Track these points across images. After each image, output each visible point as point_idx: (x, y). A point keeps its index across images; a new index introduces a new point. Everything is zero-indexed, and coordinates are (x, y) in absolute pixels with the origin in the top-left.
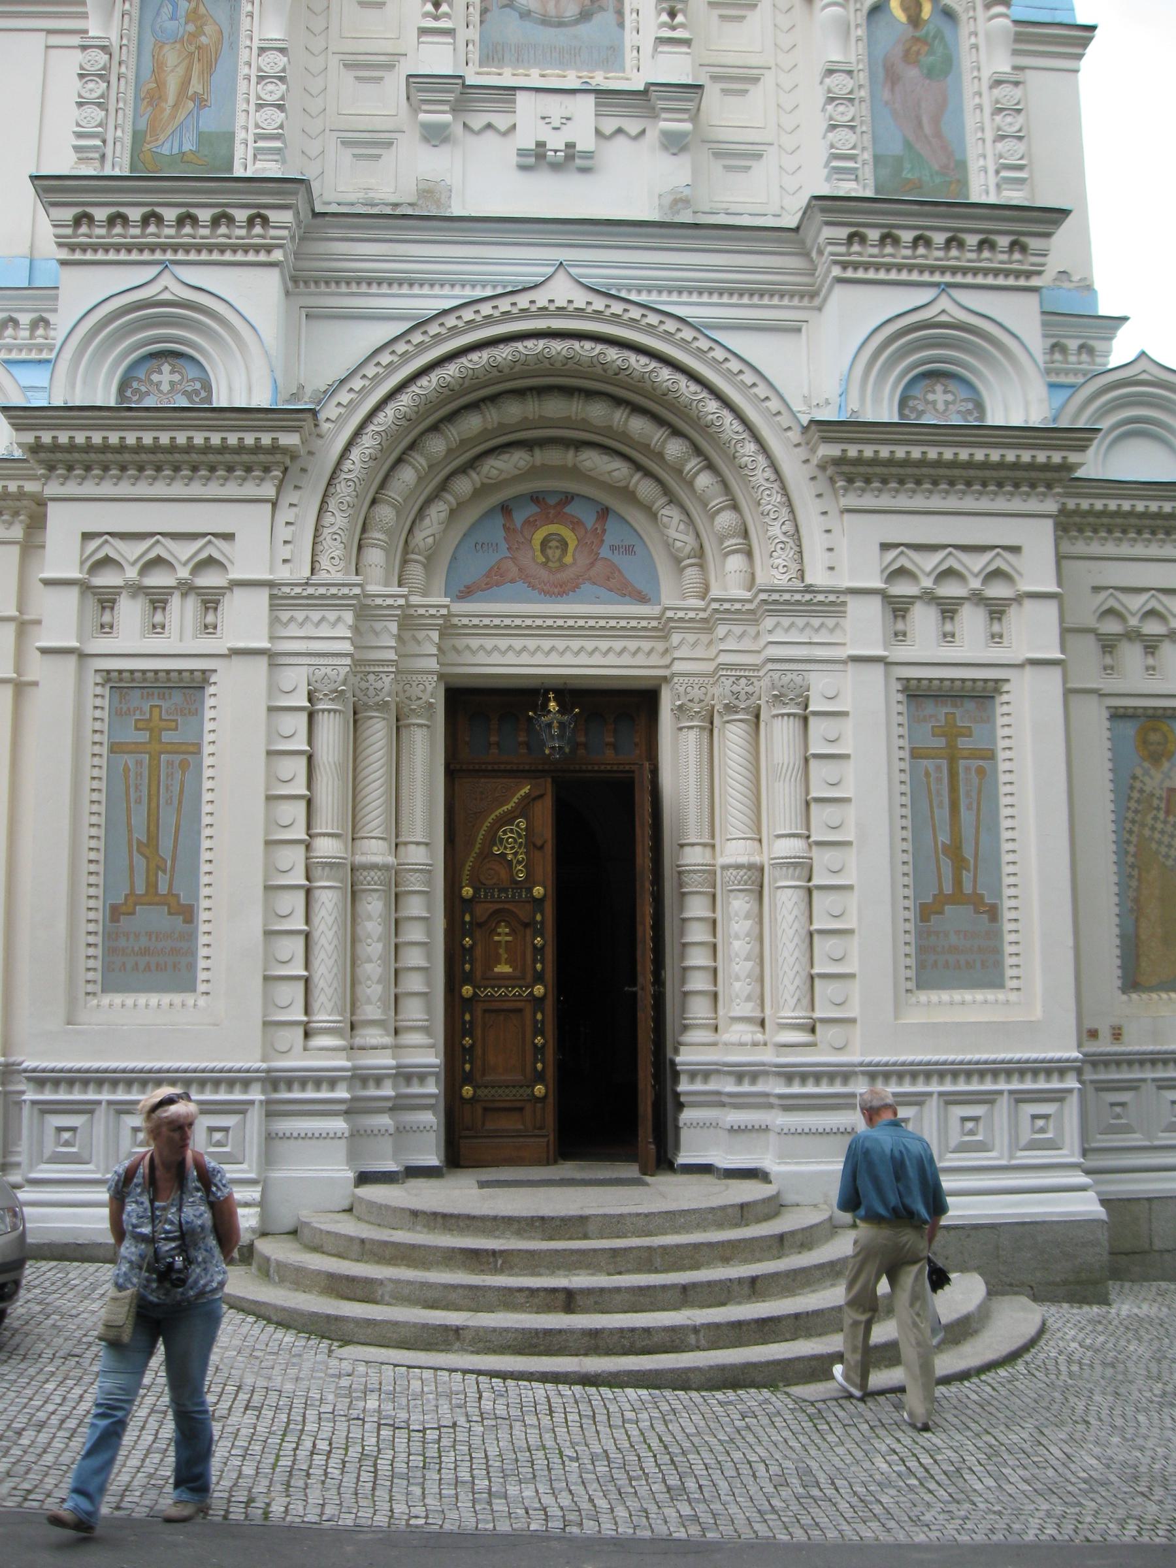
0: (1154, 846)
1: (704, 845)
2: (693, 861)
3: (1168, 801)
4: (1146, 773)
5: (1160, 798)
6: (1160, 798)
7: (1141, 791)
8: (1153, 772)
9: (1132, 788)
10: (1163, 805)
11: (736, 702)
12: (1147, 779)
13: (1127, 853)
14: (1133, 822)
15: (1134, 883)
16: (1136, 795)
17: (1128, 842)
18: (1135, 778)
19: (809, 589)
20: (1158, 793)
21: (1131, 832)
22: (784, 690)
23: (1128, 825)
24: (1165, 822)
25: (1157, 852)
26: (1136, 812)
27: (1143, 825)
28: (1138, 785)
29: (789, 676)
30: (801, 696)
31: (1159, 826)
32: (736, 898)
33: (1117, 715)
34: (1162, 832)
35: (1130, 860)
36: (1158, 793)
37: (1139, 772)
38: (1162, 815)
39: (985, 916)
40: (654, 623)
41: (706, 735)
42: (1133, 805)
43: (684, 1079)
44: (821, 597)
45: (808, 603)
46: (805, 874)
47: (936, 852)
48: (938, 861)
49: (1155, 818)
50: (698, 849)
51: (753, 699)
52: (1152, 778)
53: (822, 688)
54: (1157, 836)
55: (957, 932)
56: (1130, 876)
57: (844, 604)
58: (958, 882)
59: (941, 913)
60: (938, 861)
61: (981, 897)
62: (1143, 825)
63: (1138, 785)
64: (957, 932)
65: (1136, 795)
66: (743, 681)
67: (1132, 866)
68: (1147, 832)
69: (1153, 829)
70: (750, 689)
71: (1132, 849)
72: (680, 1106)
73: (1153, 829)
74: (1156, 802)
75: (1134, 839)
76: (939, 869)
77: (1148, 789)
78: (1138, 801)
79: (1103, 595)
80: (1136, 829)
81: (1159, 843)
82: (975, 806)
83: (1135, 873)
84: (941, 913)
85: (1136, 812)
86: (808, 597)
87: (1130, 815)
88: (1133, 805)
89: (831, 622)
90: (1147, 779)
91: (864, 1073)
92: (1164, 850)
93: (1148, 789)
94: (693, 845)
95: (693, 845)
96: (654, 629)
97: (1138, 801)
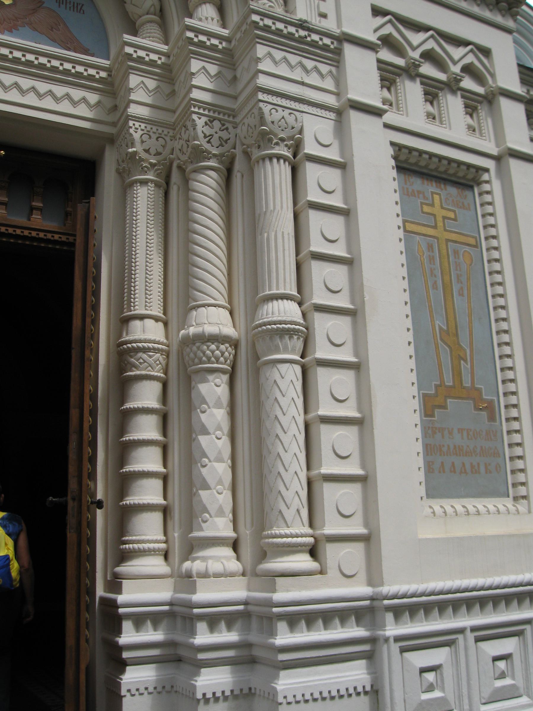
1: (157, 319)
2: (143, 337)
11: (207, 146)
19: (302, 25)
22: (275, 128)
29: (281, 113)
30: (292, 138)
32: (205, 381)
39: (484, 413)
40: (103, 74)
41: (161, 192)
43: (127, 626)
44: (315, 37)
45: (301, 40)
46: (299, 344)
47: (434, 336)
48: (437, 347)
50: (149, 323)
51: (227, 147)
53: (317, 132)
55: (460, 431)
57: (338, 52)
58: (457, 374)
59: (443, 407)
60: (437, 347)
61: (479, 390)
64: (460, 431)
66: (217, 124)
70: (224, 135)
72: (121, 665)
76: (438, 355)
82: (465, 292)
84: (443, 407)
86: (303, 33)
89: (324, 69)
91: (388, 609)
94: (142, 318)
95: (142, 318)
96: (101, 80)
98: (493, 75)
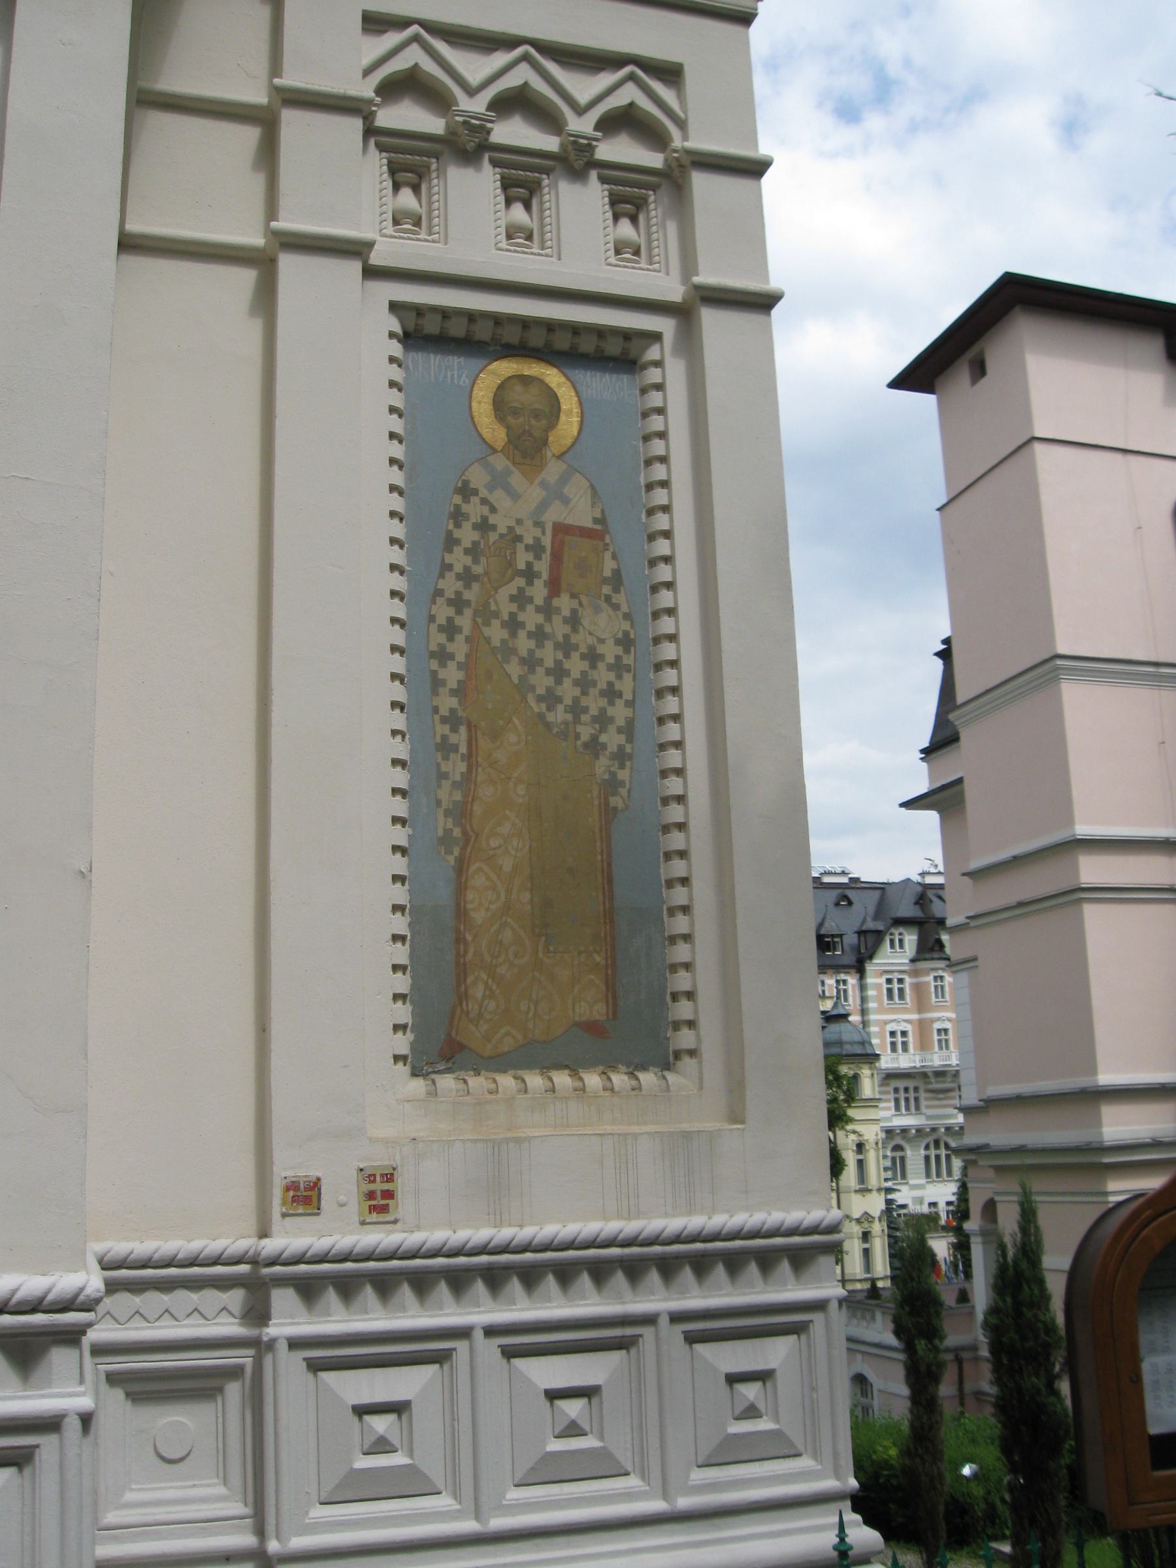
0: (514, 670)
3: (557, 557)
4: (498, 481)
5: (536, 549)
6: (536, 549)
7: (484, 526)
8: (516, 479)
9: (458, 516)
10: (543, 566)
12: (499, 497)
13: (436, 683)
14: (458, 603)
15: (457, 767)
16: (467, 535)
17: (443, 656)
18: (466, 491)
20: (529, 535)
21: (450, 629)
23: (443, 612)
24: (547, 610)
25: (524, 687)
26: (467, 577)
27: (485, 614)
28: (475, 510)
31: (531, 618)
33: (422, 332)
34: (539, 635)
35: (447, 703)
36: (529, 535)
37: (478, 477)
38: (539, 592)
42: (459, 559)
49: (521, 599)
52: (514, 496)
54: (524, 644)
56: (446, 748)
62: (485, 614)
63: (475, 510)
65: (467, 535)
67: (452, 720)
68: (496, 633)
69: (513, 625)
71: (452, 675)
73: (513, 625)
74: (523, 558)
75: (459, 648)
77: (502, 522)
78: (473, 551)
79: (392, 39)
80: (465, 622)
81: (531, 663)
83: (460, 738)
85: (467, 577)
87: (450, 585)
88: (459, 559)
90: (499, 497)
92: (542, 681)
93: (502, 522)
97: (473, 551)
98: (682, 124)
